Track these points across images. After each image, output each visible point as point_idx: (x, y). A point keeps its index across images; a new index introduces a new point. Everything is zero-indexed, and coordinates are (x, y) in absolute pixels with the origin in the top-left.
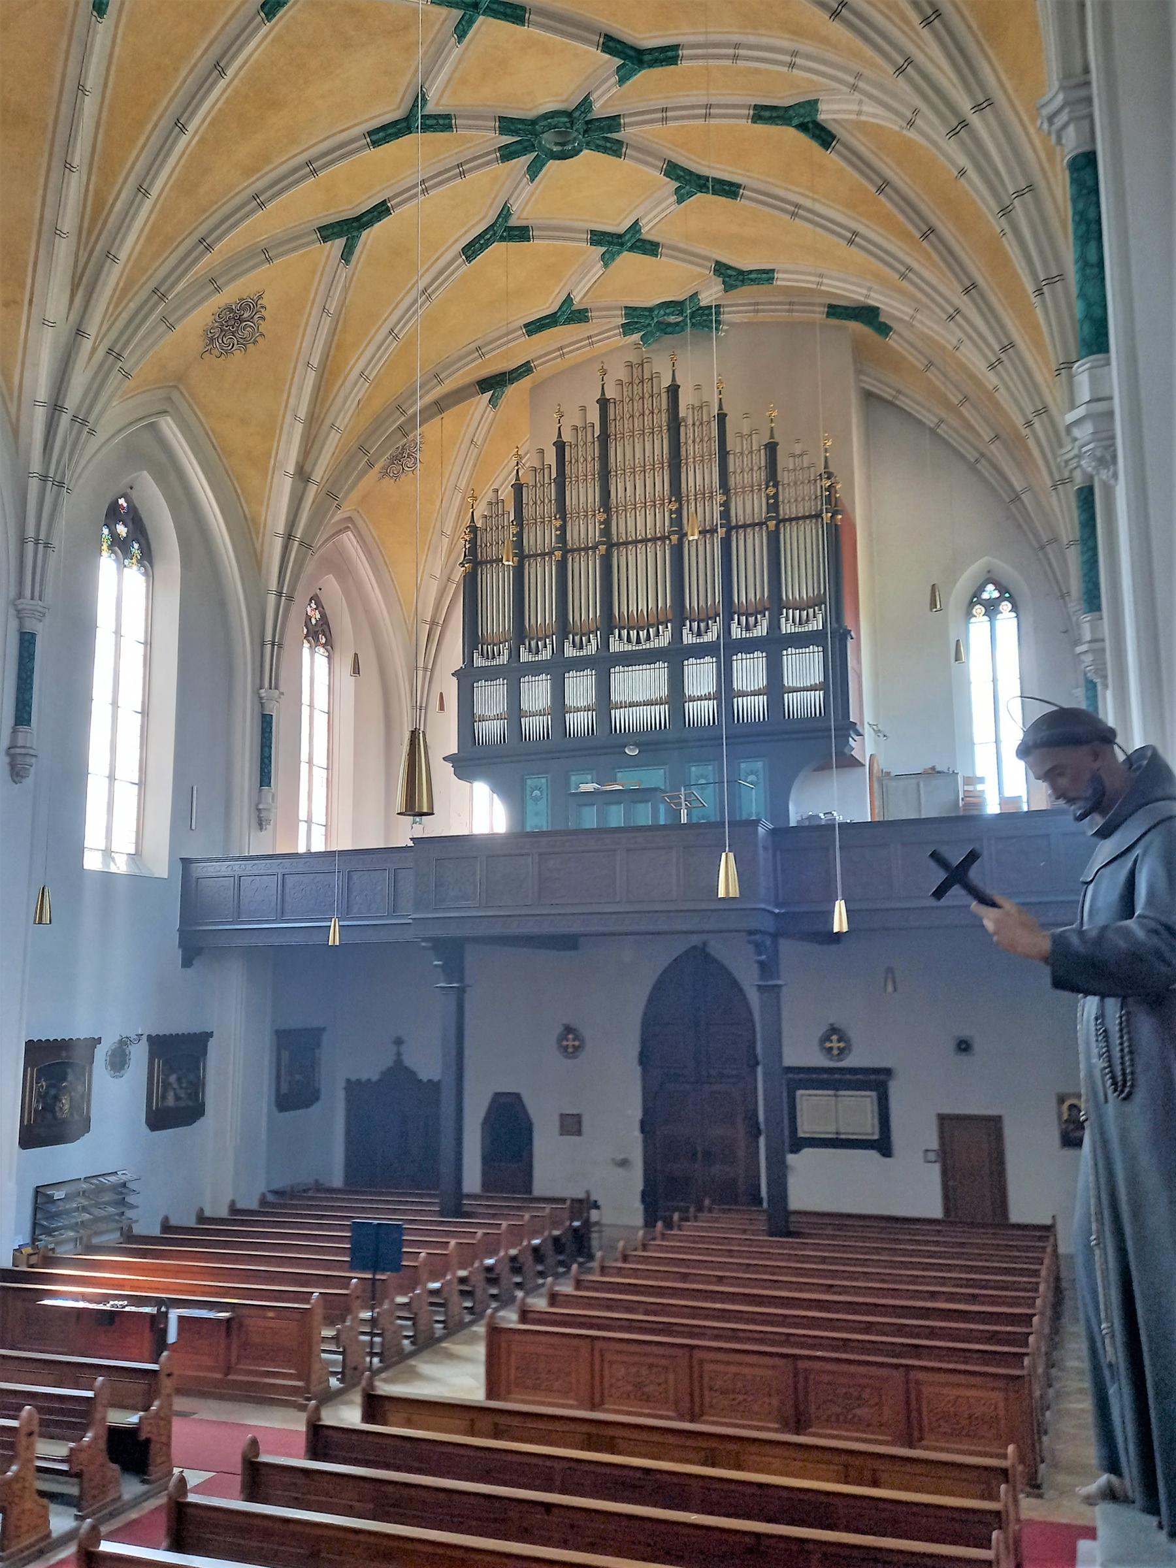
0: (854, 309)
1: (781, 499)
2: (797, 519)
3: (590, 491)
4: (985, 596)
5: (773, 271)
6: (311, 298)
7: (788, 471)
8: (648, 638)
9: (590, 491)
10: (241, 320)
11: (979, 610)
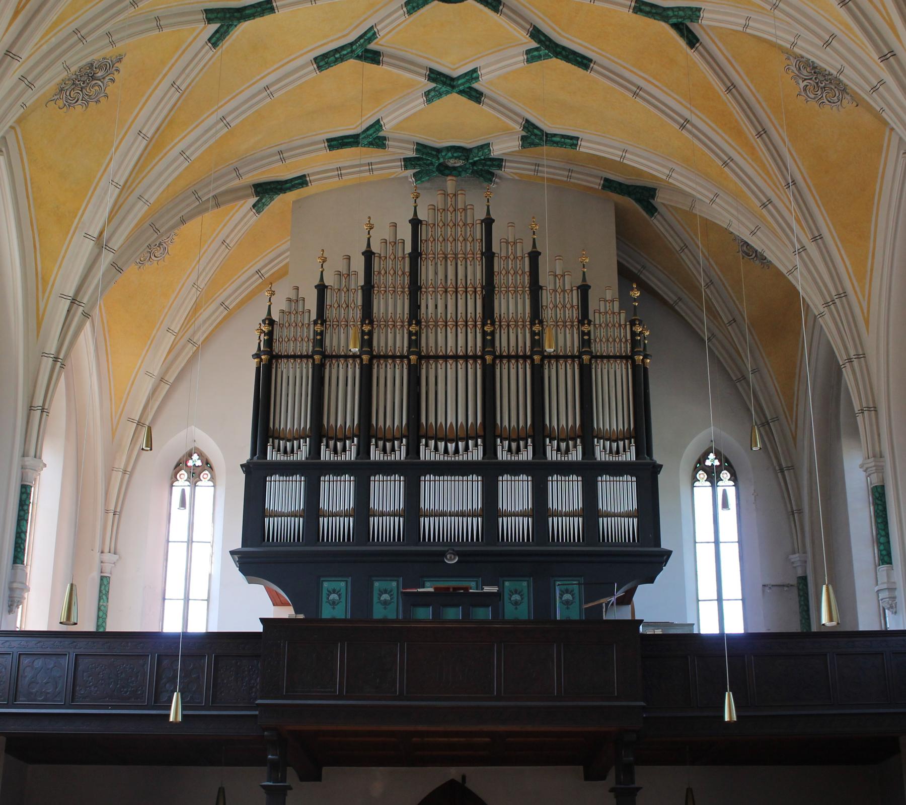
0: (628, 186)
1: (592, 337)
2: (608, 357)
3: (399, 302)
4: (708, 463)
5: (577, 138)
6: (164, 72)
7: (600, 313)
8: (457, 451)
9: (399, 302)
10: (93, 78)
11: (701, 475)
